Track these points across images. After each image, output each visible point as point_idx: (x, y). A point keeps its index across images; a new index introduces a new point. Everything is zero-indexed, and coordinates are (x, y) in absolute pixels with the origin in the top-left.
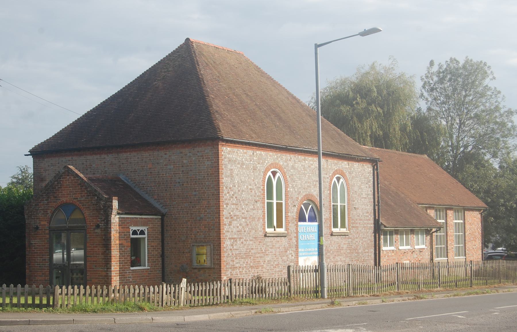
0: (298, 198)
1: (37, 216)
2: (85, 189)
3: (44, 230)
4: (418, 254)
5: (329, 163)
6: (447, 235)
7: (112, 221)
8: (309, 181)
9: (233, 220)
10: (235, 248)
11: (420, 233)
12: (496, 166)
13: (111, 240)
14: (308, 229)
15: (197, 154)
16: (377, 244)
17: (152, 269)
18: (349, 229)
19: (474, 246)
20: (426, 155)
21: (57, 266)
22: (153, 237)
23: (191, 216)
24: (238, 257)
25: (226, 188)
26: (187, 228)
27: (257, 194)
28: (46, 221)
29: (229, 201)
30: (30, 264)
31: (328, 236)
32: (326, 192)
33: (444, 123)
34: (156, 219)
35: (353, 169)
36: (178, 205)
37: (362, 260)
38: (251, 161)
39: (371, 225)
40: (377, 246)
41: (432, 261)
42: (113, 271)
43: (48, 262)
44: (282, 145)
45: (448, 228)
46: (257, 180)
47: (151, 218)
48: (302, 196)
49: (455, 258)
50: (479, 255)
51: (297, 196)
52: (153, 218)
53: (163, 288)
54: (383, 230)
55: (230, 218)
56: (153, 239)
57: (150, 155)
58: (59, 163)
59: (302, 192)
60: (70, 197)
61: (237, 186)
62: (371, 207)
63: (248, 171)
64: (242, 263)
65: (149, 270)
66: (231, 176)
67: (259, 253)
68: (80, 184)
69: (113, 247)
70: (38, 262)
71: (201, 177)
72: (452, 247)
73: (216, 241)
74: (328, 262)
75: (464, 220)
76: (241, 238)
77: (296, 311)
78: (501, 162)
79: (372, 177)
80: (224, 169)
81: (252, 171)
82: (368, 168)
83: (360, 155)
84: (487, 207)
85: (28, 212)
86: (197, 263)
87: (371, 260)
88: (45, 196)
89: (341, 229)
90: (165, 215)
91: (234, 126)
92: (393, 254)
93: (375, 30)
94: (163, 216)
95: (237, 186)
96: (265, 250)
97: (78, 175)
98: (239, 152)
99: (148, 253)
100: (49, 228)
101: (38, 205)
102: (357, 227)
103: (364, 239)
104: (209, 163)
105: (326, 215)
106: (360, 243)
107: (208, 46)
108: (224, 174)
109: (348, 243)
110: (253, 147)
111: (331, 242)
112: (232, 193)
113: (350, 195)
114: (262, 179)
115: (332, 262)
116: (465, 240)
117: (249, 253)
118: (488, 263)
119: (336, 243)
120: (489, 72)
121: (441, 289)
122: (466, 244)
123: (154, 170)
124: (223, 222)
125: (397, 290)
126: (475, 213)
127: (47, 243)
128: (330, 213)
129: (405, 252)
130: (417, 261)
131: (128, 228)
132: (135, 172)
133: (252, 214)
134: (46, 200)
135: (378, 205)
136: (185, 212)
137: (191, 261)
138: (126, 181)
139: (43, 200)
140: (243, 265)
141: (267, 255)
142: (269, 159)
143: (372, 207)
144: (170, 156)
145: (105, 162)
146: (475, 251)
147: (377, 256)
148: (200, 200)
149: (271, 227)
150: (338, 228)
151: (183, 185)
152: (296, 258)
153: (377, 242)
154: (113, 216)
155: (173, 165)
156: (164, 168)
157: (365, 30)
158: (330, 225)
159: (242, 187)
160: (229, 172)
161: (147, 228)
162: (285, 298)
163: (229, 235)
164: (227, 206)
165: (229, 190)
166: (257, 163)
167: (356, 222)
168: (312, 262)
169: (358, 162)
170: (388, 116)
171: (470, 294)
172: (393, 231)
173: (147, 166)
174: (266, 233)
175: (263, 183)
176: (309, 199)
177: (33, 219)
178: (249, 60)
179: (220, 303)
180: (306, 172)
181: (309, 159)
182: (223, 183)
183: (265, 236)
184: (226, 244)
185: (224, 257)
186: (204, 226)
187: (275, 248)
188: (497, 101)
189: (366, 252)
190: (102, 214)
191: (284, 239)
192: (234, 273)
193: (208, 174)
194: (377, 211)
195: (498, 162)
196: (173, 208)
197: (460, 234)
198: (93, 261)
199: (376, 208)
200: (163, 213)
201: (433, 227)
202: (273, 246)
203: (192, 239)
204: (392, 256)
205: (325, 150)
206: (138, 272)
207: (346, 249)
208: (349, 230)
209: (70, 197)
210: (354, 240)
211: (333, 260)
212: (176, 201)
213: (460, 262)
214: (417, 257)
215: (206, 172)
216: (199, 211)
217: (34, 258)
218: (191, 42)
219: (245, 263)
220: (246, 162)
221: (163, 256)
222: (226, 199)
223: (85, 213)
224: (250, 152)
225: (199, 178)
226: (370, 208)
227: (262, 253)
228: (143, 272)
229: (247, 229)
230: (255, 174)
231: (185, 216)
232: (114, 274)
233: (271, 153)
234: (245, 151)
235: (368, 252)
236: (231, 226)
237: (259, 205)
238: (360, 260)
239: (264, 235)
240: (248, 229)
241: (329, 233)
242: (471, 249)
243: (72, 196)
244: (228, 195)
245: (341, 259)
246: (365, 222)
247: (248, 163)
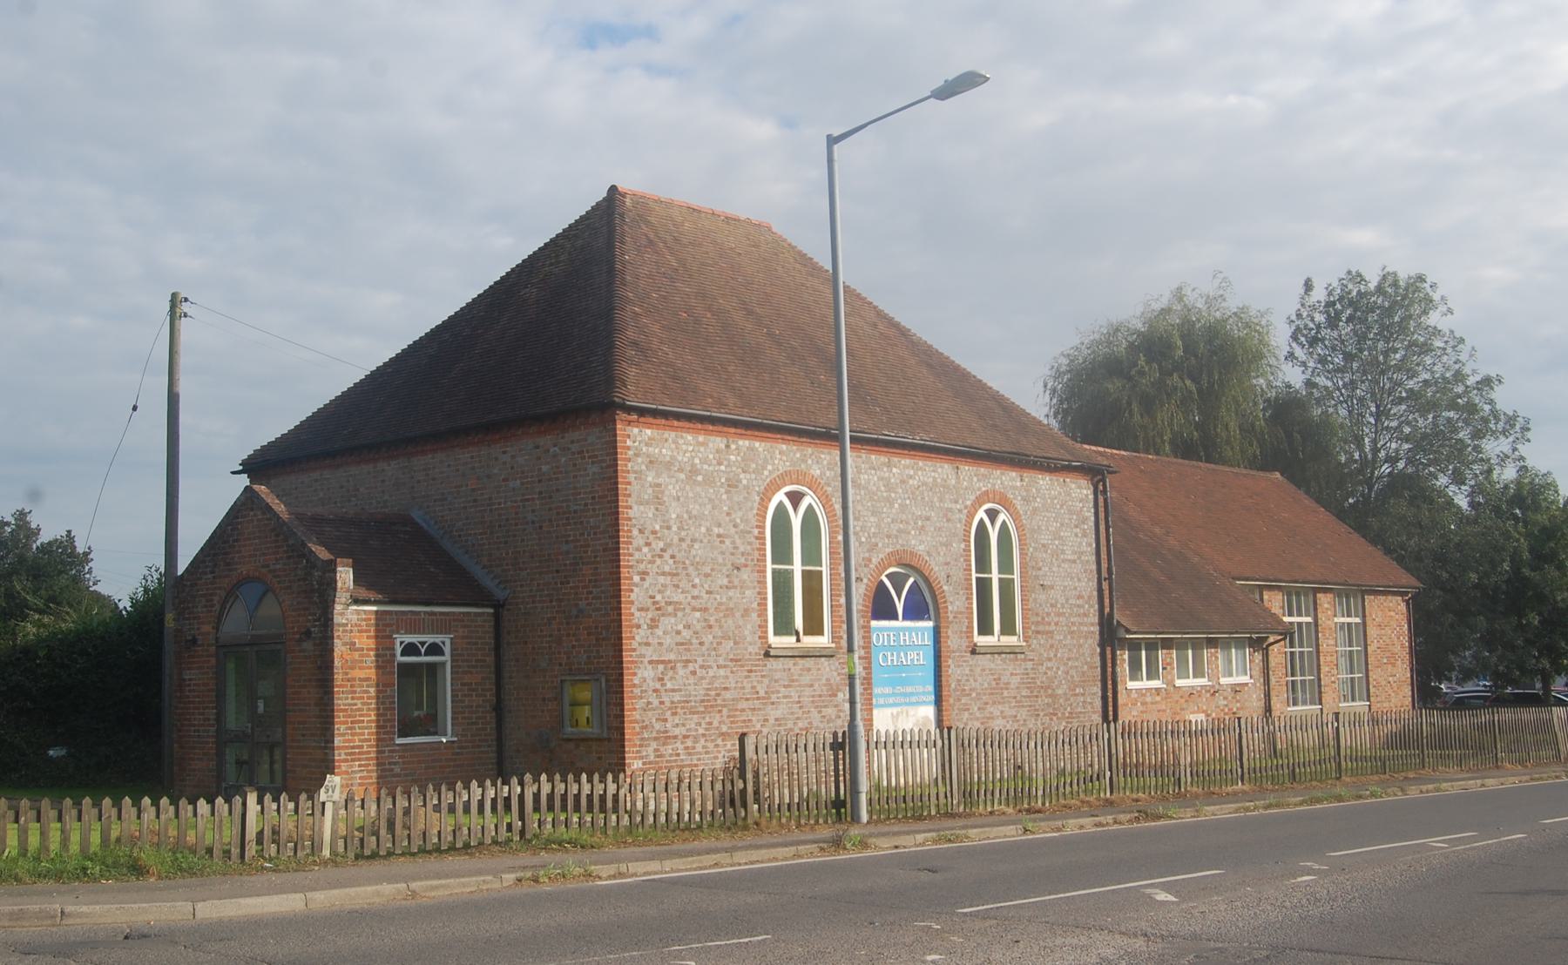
0: (870, 560)
4: (1230, 698)
5: (964, 474)
6: (1318, 652)
7: (335, 621)
8: (904, 517)
9: (663, 615)
10: (669, 685)
11: (1233, 645)
12: (1462, 502)
13: (332, 667)
14: (902, 638)
15: (569, 449)
16: (1109, 674)
18: (1024, 637)
19: (1391, 676)
20: (1277, 473)
22: (467, 661)
24: (679, 710)
25: (641, 531)
26: (551, 636)
27: (742, 549)
29: (650, 566)
30: (180, 731)
31: (962, 657)
32: (954, 545)
33: (1343, 412)
35: (1034, 490)
36: (532, 580)
37: (1067, 715)
38: (720, 464)
39: (1092, 629)
40: (1109, 678)
41: (1268, 714)
42: (339, 748)
43: (213, 725)
44: (813, 426)
45: (1320, 635)
46: (740, 514)
47: (460, 613)
48: (881, 556)
49: (1340, 705)
50: (1404, 697)
51: (867, 555)
52: (468, 613)
53: (244, 804)
54: (1121, 638)
56: (468, 666)
57: (472, 457)
59: (880, 545)
61: (674, 528)
62: (1091, 584)
63: (712, 491)
64: (693, 726)
65: (456, 745)
66: (658, 500)
67: (747, 699)
69: (338, 686)
70: (194, 725)
71: (580, 505)
72: (1333, 679)
74: (965, 720)
75: (1364, 616)
76: (688, 661)
77: (690, 870)
78: (1471, 495)
79: (1093, 510)
81: (723, 490)
82: (1080, 491)
83: (1056, 456)
84: (1422, 585)
86: (572, 727)
87: (1094, 712)
89: (1002, 637)
91: (675, 378)
92: (1158, 698)
93: (969, 81)
94: (498, 606)
95: (674, 528)
96: (766, 693)
97: (270, 507)
98: (681, 441)
100: (217, 639)
101: (196, 584)
102: (1052, 632)
103: (1070, 663)
104: (595, 469)
105: (957, 603)
106: (1060, 673)
107: (669, 204)
109: (1023, 671)
110: (725, 429)
111: (971, 670)
112: (661, 544)
113: (1027, 554)
114: (755, 512)
115: (978, 719)
116: (1367, 664)
117: (716, 700)
118: (1449, 716)
119: (987, 672)
120: (1436, 297)
121: (1246, 787)
122: (1371, 674)
123: (482, 494)
125: (1108, 794)
126: (1391, 602)
128: (969, 598)
129: (1191, 694)
130: (1225, 714)
131: (390, 637)
133: (724, 600)
135: (1109, 578)
138: (423, 524)
139: (206, 573)
140: (697, 730)
141: (773, 703)
142: (776, 462)
143: (1095, 584)
145: (383, 481)
146: (1395, 689)
147: (1111, 704)
148: (578, 564)
149: (791, 634)
150: (993, 634)
151: (541, 527)
152: (866, 710)
153: (1110, 670)
154: (338, 608)
157: (946, 81)
158: (970, 627)
159: (693, 529)
160: (650, 491)
161: (452, 639)
162: (716, 824)
163: (649, 653)
164: (643, 579)
165: (651, 537)
166: (740, 470)
167: (1046, 619)
168: (918, 721)
169: (1051, 472)
170: (1209, 398)
171: (1319, 801)
172: (1157, 643)
173: (467, 485)
174: (770, 647)
175: (758, 520)
176: (904, 562)
178: (785, 240)
179: (481, 843)
180: (893, 495)
181: (903, 462)
182: (630, 519)
183: (767, 655)
184: (641, 676)
187: (800, 686)
188: (1458, 360)
189: (1076, 695)
191: (826, 663)
192: (668, 750)
193: (593, 498)
194: (1106, 593)
195: (1466, 493)
196: (522, 586)
197: (1355, 648)
199: (1105, 585)
200: (499, 601)
201: (1271, 633)
202: (793, 681)
203: (560, 665)
204: (1156, 703)
205: (948, 442)
207: (1018, 688)
208: (1027, 642)
209: (255, 563)
210: (1042, 665)
211: (978, 715)
213: (1304, 718)
214: (1226, 706)
215: (590, 492)
218: (620, 194)
219: (704, 726)
220: (706, 467)
221: (499, 709)
223: (284, 601)
224: (718, 442)
225: (575, 508)
226: (1088, 586)
227: (758, 698)
229: (708, 639)
230: (736, 499)
231: (547, 607)
232: (343, 757)
233: (784, 447)
234: (701, 438)
235: (1083, 695)
236: (657, 630)
237: (745, 577)
238: (1060, 715)
239: (763, 652)
240: (710, 637)
241: (968, 647)
242: (1384, 683)
244: (645, 550)
245: (1002, 712)
246: (1072, 620)
247: (711, 468)
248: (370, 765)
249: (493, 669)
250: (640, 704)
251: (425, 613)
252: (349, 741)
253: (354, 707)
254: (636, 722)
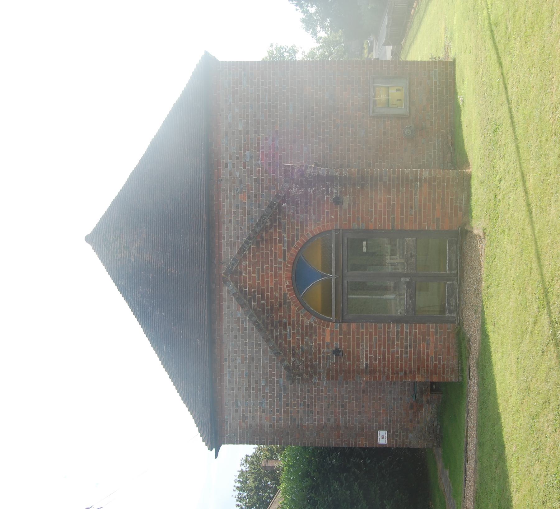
1: (315, 353)
2: (267, 232)
3: (341, 334)
21: (410, 306)
28: (324, 331)
58: (233, 389)
60: (280, 269)
68: (258, 243)
70: (402, 351)
85: (307, 374)
88: (277, 331)
127: (367, 328)
134: (285, 328)
137: (399, 117)
139: (285, 335)
144: (230, 158)
155: (245, 151)
156: (248, 169)
173: (245, 203)
177: (320, 362)
190: (315, 191)
198: (402, 214)
209: (280, 269)
217: (393, 360)
223: (311, 232)
243: (280, 263)
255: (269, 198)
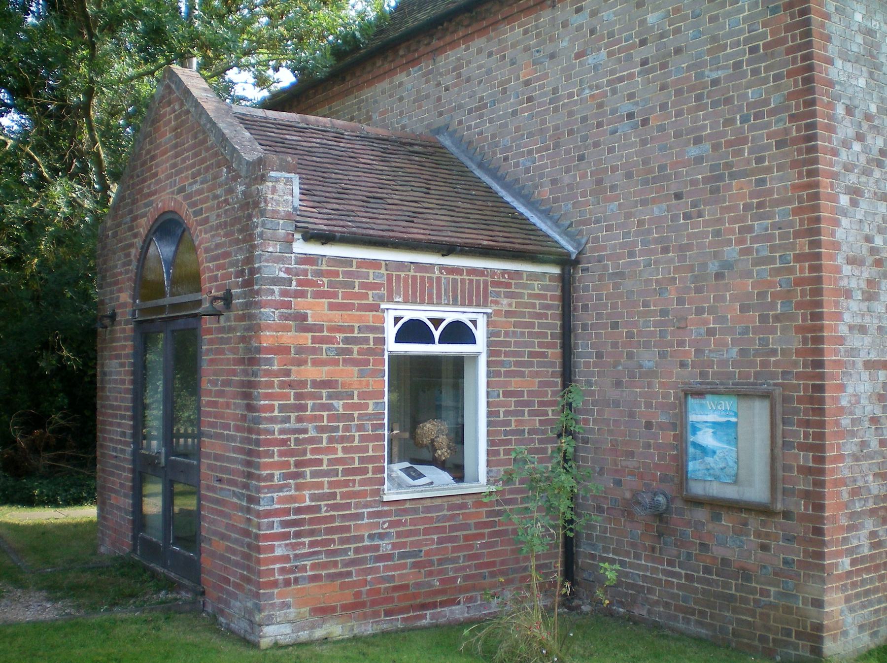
17: (511, 491)
22: (514, 354)
23: (682, 258)
25: (849, 111)
29: (863, 179)
34: (532, 276)
36: (628, 216)
47: (504, 272)
52: (517, 272)
55: (870, 260)
56: (517, 364)
57: (526, 32)
71: (725, 67)
73: (799, 376)
80: (835, 18)
90: (577, 262)
99: (489, 424)
108: (836, 41)
124: (836, 280)
131: (375, 308)
132: (478, 109)
136: (656, 241)
144: (594, 14)
148: (720, 178)
151: (645, 122)
164: (854, 203)
165: (865, 126)
182: (831, 84)
185: (840, 458)
186: (737, 305)
196: (609, 228)
203: (683, 365)
206: (428, 509)
212: (617, 198)
216: (717, 233)
222: (848, 168)
225: (715, 75)
228: (463, 506)
231: (657, 262)
232: (277, 530)
244: (857, 147)
248: (333, 541)
249: (558, 369)
250: (850, 447)
251: (442, 267)
252: (292, 499)
253: (301, 436)
254: (842, 482)
255: (527, 133)
